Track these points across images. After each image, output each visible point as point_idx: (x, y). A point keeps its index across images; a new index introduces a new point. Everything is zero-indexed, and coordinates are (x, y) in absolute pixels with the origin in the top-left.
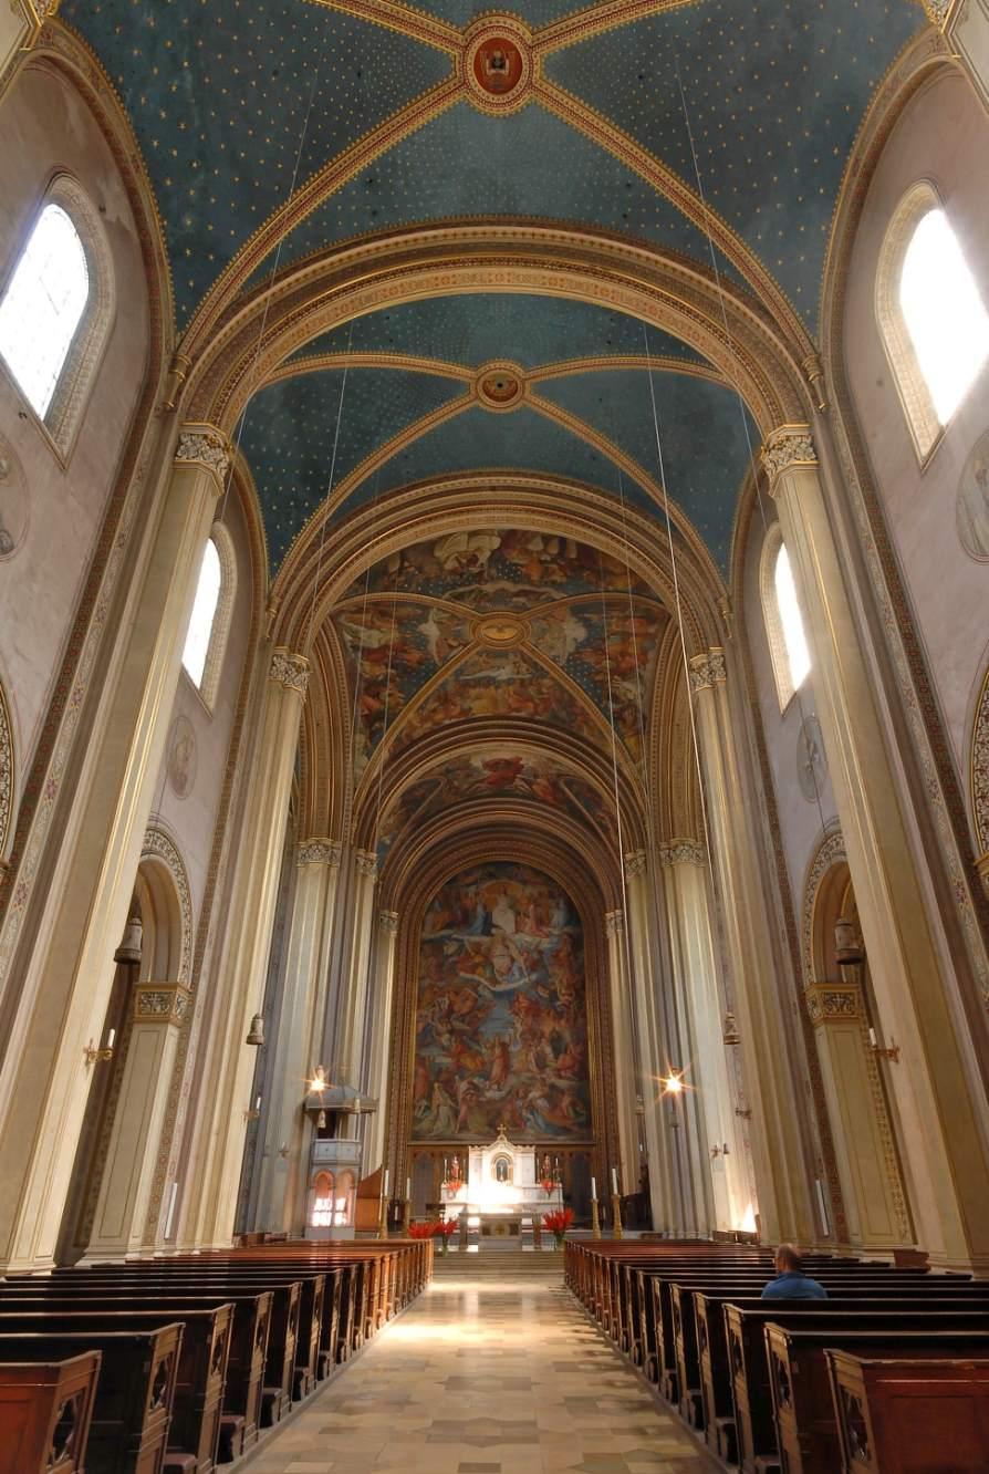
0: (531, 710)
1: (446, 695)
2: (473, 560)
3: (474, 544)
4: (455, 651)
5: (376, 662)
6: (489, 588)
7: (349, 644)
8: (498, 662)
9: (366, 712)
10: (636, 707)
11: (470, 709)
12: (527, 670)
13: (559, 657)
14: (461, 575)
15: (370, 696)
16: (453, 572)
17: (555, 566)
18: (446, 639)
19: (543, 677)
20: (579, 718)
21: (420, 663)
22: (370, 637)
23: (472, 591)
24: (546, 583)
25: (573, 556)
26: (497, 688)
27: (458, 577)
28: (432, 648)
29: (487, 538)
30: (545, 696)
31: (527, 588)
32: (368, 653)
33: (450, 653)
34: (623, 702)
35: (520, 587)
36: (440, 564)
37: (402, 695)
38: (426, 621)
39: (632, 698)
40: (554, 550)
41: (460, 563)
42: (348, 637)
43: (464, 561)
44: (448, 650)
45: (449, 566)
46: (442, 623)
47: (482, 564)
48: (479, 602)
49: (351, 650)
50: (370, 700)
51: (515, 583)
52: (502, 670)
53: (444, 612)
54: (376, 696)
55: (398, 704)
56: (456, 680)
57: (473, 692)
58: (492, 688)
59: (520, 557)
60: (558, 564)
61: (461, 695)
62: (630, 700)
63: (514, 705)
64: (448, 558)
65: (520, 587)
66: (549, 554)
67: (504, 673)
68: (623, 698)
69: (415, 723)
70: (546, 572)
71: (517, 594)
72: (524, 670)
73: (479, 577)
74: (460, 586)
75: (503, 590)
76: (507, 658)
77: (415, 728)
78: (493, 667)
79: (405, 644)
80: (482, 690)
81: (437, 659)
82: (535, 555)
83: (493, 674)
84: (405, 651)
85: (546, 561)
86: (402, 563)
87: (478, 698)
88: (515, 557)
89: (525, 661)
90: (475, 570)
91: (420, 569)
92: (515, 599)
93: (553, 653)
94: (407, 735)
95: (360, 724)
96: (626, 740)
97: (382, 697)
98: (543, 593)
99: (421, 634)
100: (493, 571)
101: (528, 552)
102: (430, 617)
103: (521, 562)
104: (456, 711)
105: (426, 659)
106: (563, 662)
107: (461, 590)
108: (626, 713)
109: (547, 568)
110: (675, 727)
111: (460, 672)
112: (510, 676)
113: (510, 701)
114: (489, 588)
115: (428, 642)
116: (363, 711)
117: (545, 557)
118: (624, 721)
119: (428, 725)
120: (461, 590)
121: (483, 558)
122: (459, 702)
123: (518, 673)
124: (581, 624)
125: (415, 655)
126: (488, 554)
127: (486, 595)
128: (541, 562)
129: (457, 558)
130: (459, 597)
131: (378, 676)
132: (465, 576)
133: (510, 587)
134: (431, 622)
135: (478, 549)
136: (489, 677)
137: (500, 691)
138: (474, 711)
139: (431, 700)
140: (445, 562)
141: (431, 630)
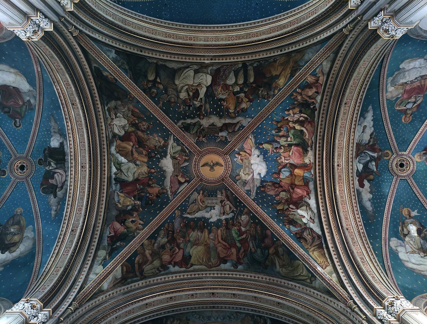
0: (234, 257)
1: (173, 232)
2: (196, 94)
3: (197, 81)
4: (183, 186)
5: (128, 194)
6: (205, 123)
7: (114, 176)
8: (209, 201)
9: (113, 234)
10: (312, 229)
11: (190, 256)
12: (230, 208)
13: (250, 191)
14: (190, 106)
15: (118, 222)
16: (184, 102)
17: (242, 95)
18: (177, 176)
19: (241, 213)
20: (271, 250)
21: (157, 196)
22: (128, 169)
23: (195, 124)
24: (238, 112)
25: (252, 80)
26: (210, 232)
27: (187, 108)
28: (168, 183)
29: (204, 75)
30: (244, 236)
31: (228, 121)
32: (123, 184)
33: (178, 189)
34: (301, 226)
35: (223, 121)
36: (178, 92)
37: (142, 222)
38: (165, 156)
39: (306, 222)
40: (241, 82)
41: (189, 95)
42: (114, 170)
43: (191, 94)
44: (178, 186)
45: (183, 95)
46: (176, 159)
47: (201, 99)
48: (199, 137)
49: (114, 182)
50: (117, 225)
51: (221, 117)
52: (212, 211)
53: (178, 145)
54: (122, 222)
55: (137, 229)
56: (181, 217)
57: (194, 235)
58: (206, 230)
59: (223, 92)
60: (245, 93)
61: (184, 237)
62: (305, 224)
63: (222, 255)
64: (182, 87)
65: (223, 121)
66: (238, 85)
67: (213, 215)
68: (298, 222)
69: (147, 252)
70: (239, 102)
71: (221, 129)
72: (228, 206)
73: (199, 112)
74: (189, 117)
75: (213, 125)
76: (216, 196)
77: (146, 262)
78: (207, 207)
79: (150, 179)
80: (199, 234)
81: (169, 193)
82: (231, 87)
83: (207, 215)
84: (149, 186)
85: (238, 93)
86: (156, 78)
87: (196, 243)
88: (221, 94)
89: (228, 199)
90: (197, 104)
91: (166, 89)
92: (220, 134)
93: (246, 188)
94: (140, 265)
95: (105, 243)
96: (311, 253)
97: (126, 224)
98: (236, 124)
99: (161, 168)
100: (208, 106)
101: (226, 87)
102: (169, 151)
103: (224, 97)
104: (179, 258)
105: (164, 193)
106: (254, 194)
107: (189, 121)
108: (305, 234)
109: (238, 98)
110: (345, 230)
111: (183, 208)
112: (218, 218)
113: (220, 249)
114: (205, 123)
115: (165, 177)
116: (110, 233)
117: (237, 89)
118: (306, 240)
119: (157, 263)
120: (189, 121)
121: (203, 92)
122: (182, 245)
123: (224, 214)
124: (262, 157)
125: (155, 189)
126: (204, 90)
127: (203, 130)
128: (235, 93)
129: (187, 91)
130: (187, 128)
131: (128, 206)
132: (191, 108)
133: (218, 122)
134: (169, 156)
135: (200, 85)
136: (204, 218)
137: (212, 236)
138: (192, 261)
139: (162, 233)
140: (180, 92)
141: (167, 164)
